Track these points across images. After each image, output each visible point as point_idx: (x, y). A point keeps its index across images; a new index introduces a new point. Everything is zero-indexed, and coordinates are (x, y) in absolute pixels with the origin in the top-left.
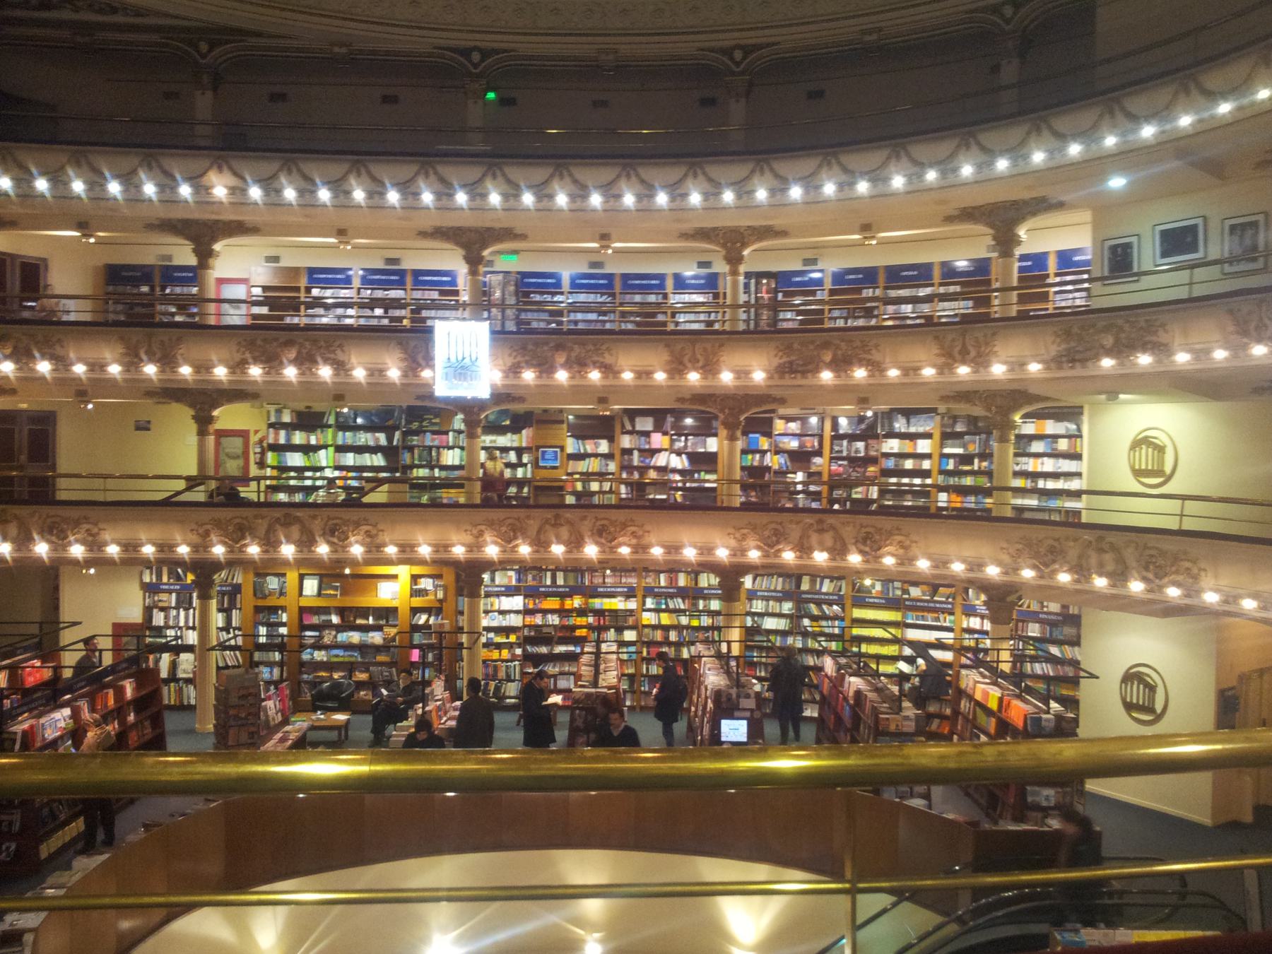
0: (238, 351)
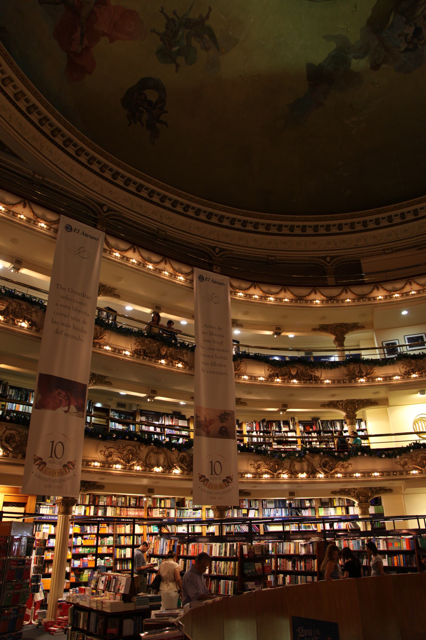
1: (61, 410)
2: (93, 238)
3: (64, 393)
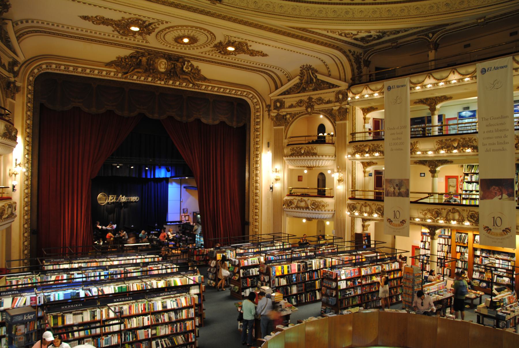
0: (437, 145)
1: (496, 199)
2: (502, 67)
3: (497, 188)
